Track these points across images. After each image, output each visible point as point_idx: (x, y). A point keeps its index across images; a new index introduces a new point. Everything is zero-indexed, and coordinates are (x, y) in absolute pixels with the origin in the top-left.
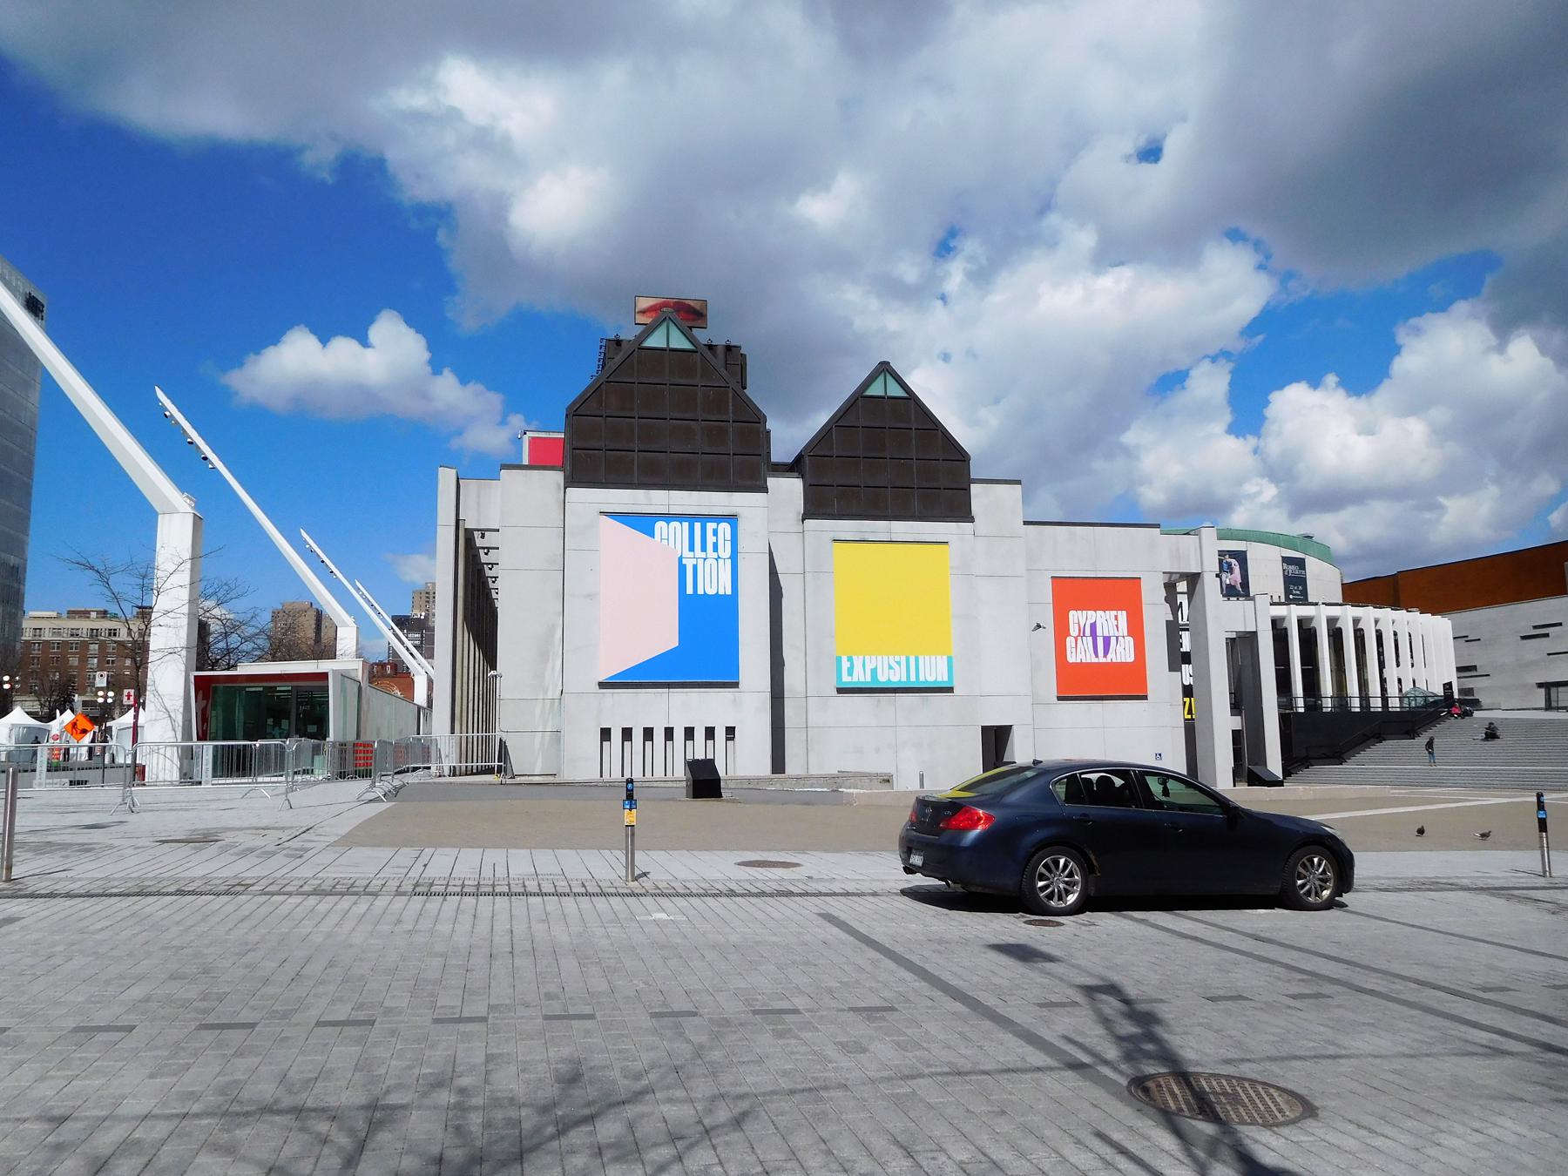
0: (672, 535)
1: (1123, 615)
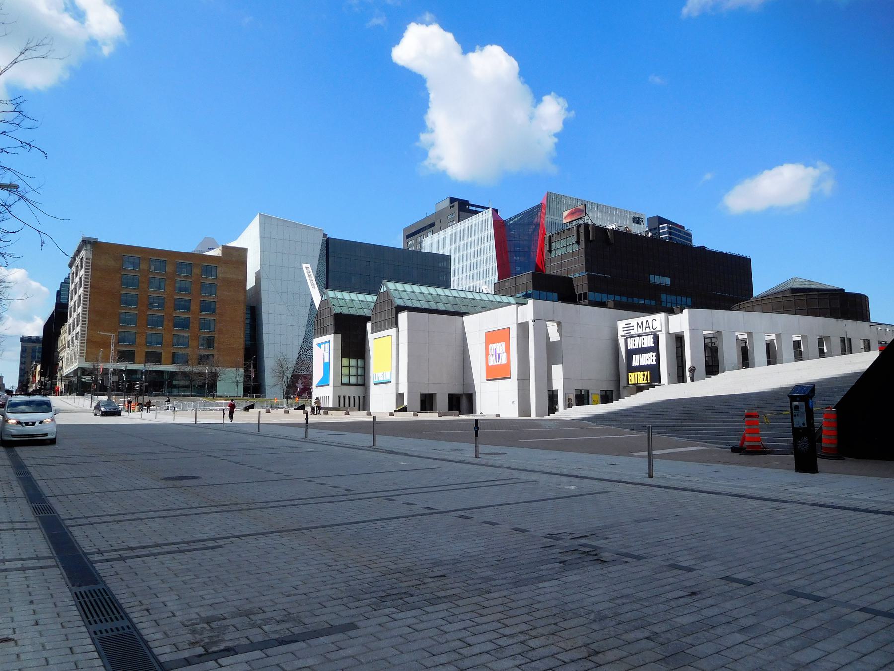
0: (323, 346)
1: (503, 344)
